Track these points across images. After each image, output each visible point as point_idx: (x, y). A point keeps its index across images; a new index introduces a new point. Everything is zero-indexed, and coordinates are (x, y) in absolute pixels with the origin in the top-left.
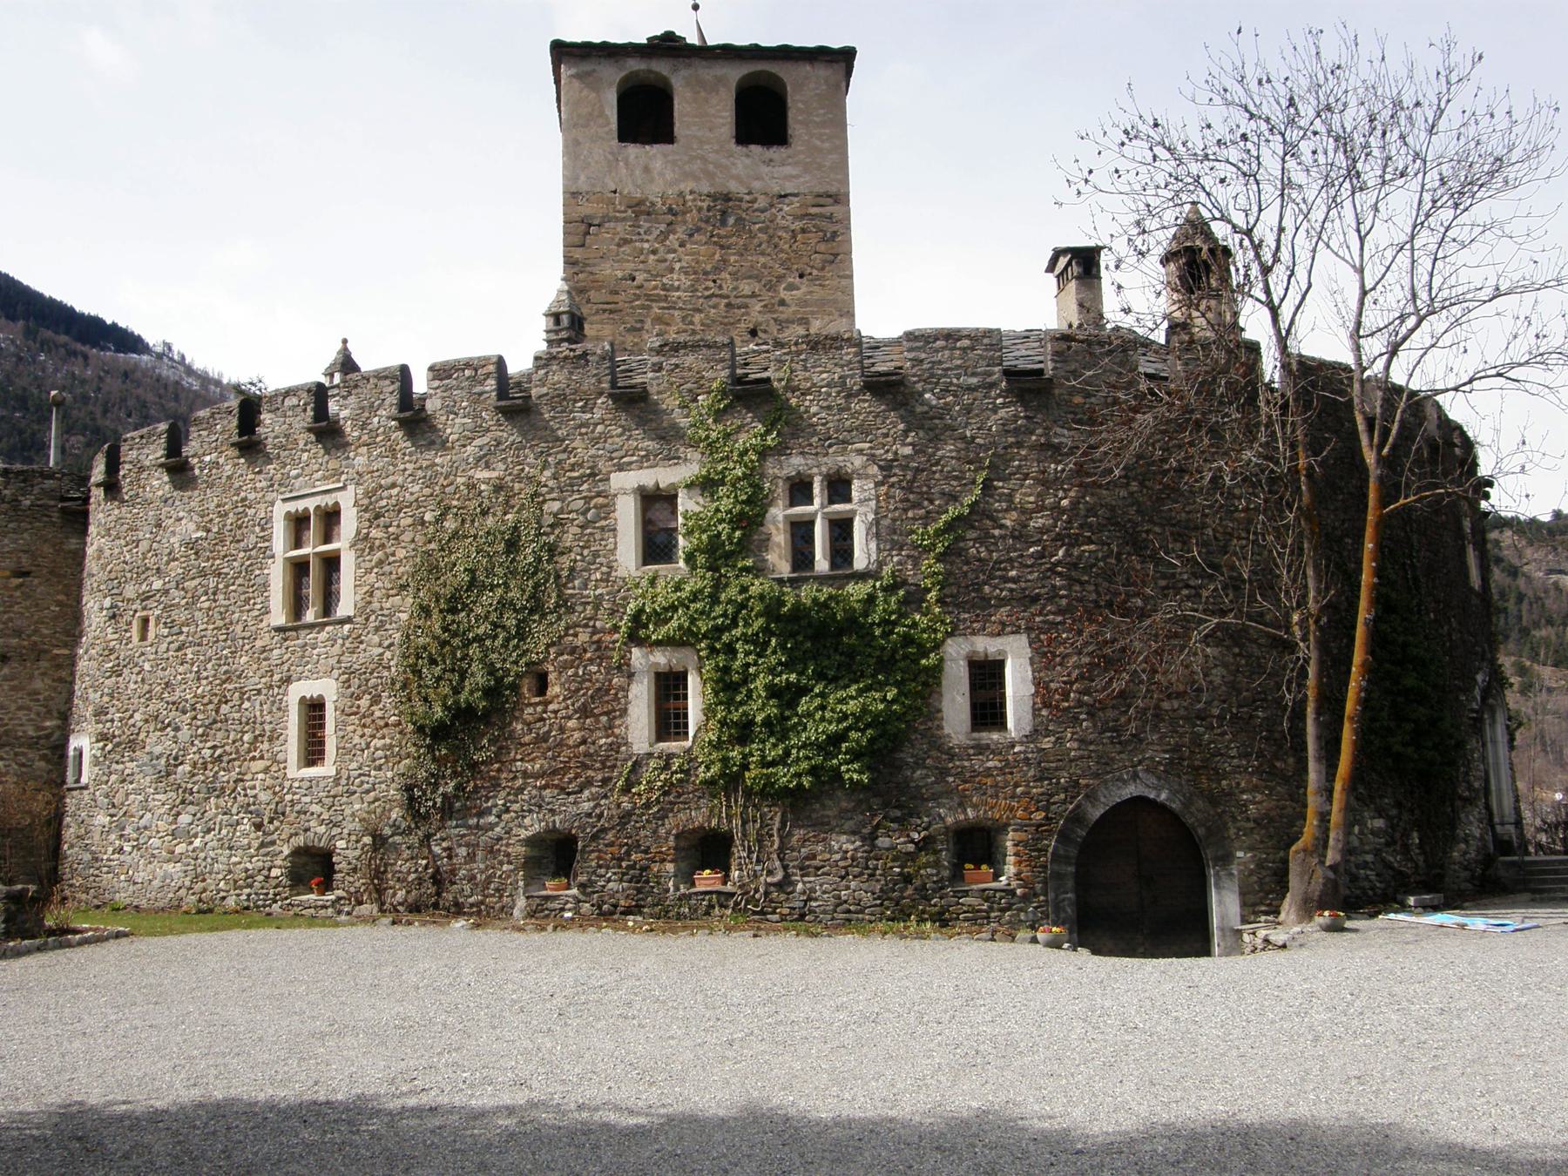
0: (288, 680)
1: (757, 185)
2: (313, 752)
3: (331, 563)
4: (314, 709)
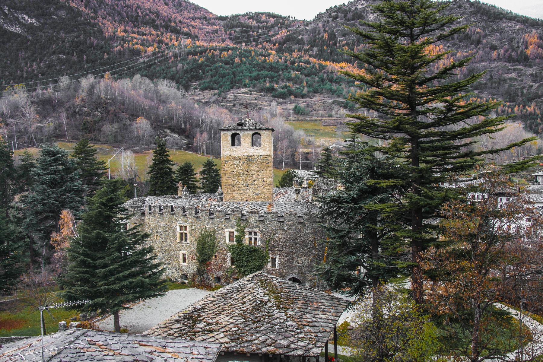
0: (180, 250)
1: (255, 154)
2: (184, 261)
3: (186, 234)
4: (184, 255)
